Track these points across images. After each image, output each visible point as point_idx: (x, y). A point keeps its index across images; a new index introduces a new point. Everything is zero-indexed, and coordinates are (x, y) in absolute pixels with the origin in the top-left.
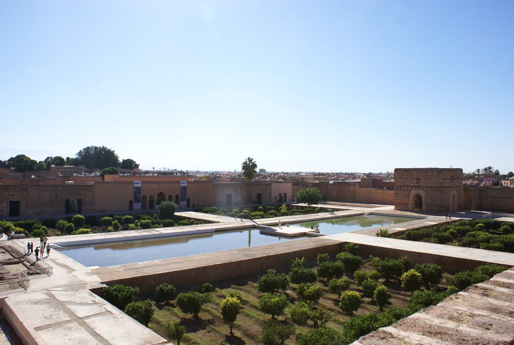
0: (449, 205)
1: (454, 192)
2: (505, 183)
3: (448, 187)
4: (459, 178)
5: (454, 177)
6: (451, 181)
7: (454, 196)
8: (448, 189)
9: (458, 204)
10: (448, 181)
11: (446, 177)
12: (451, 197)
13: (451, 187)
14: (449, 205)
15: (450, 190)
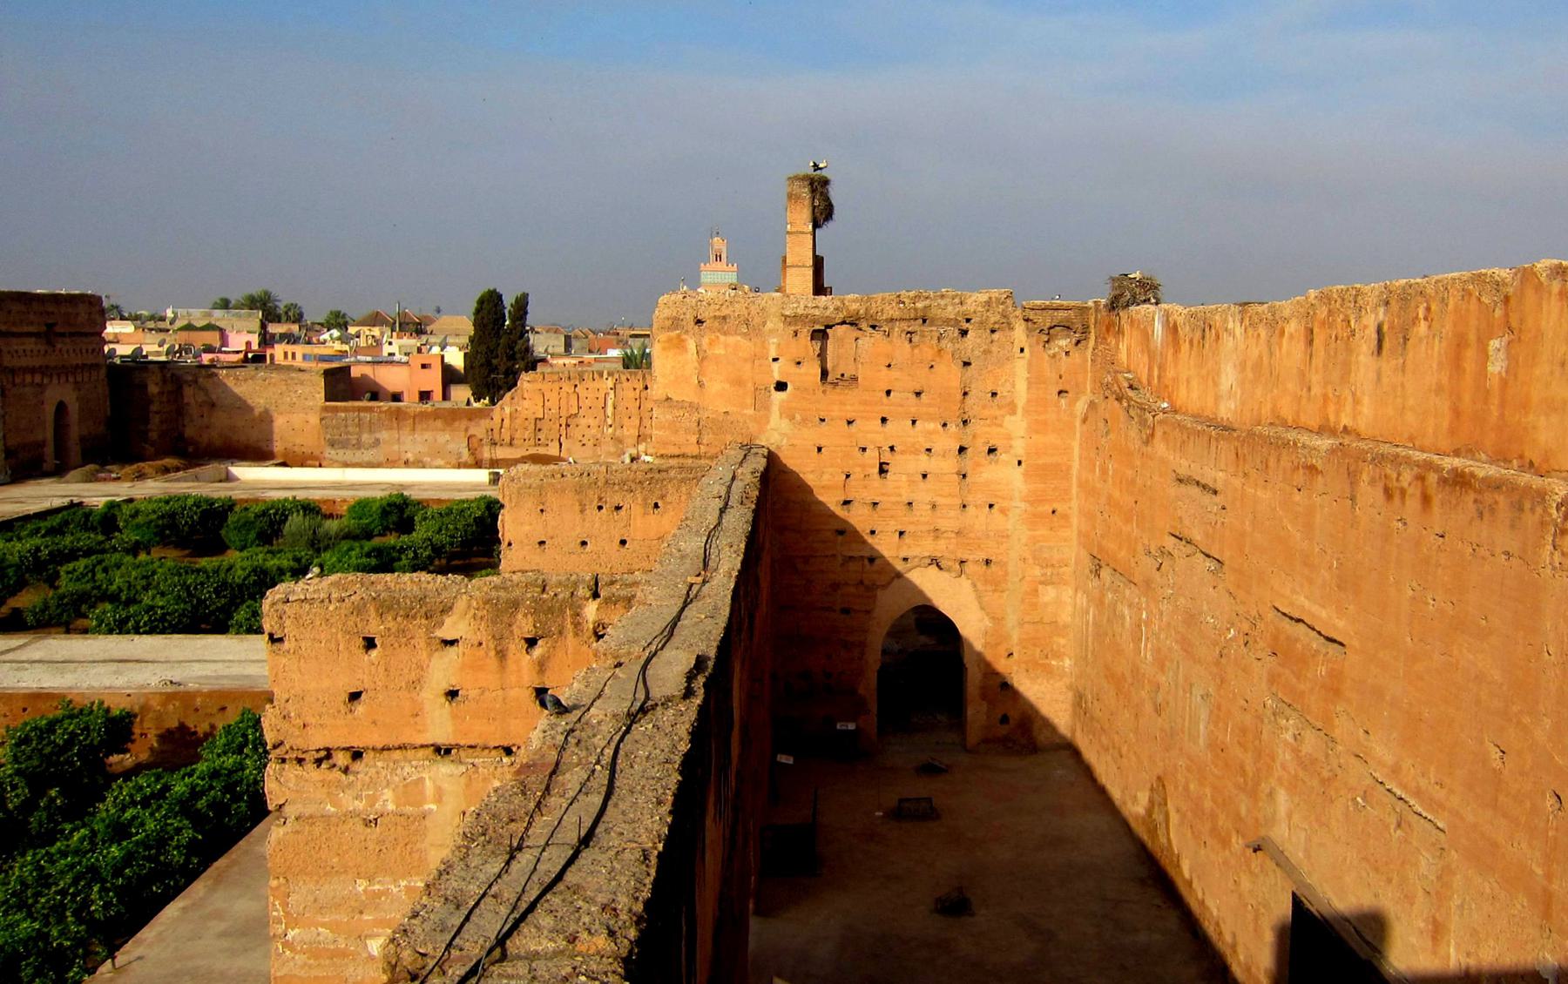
0: (43, 444)
1: (59, 392)
2: (286, 354)
3: (33, 371)
4: (86, 335)
5: (58, 329)
6: (42, 348)
7: (61, 409)
8: (28, 378)
9: (82, 439)
10: (30, 344)
11: (14, 330)
12: (50, 410)
13: (44, 370)
14: (43, 444)
15: (40, 385)
